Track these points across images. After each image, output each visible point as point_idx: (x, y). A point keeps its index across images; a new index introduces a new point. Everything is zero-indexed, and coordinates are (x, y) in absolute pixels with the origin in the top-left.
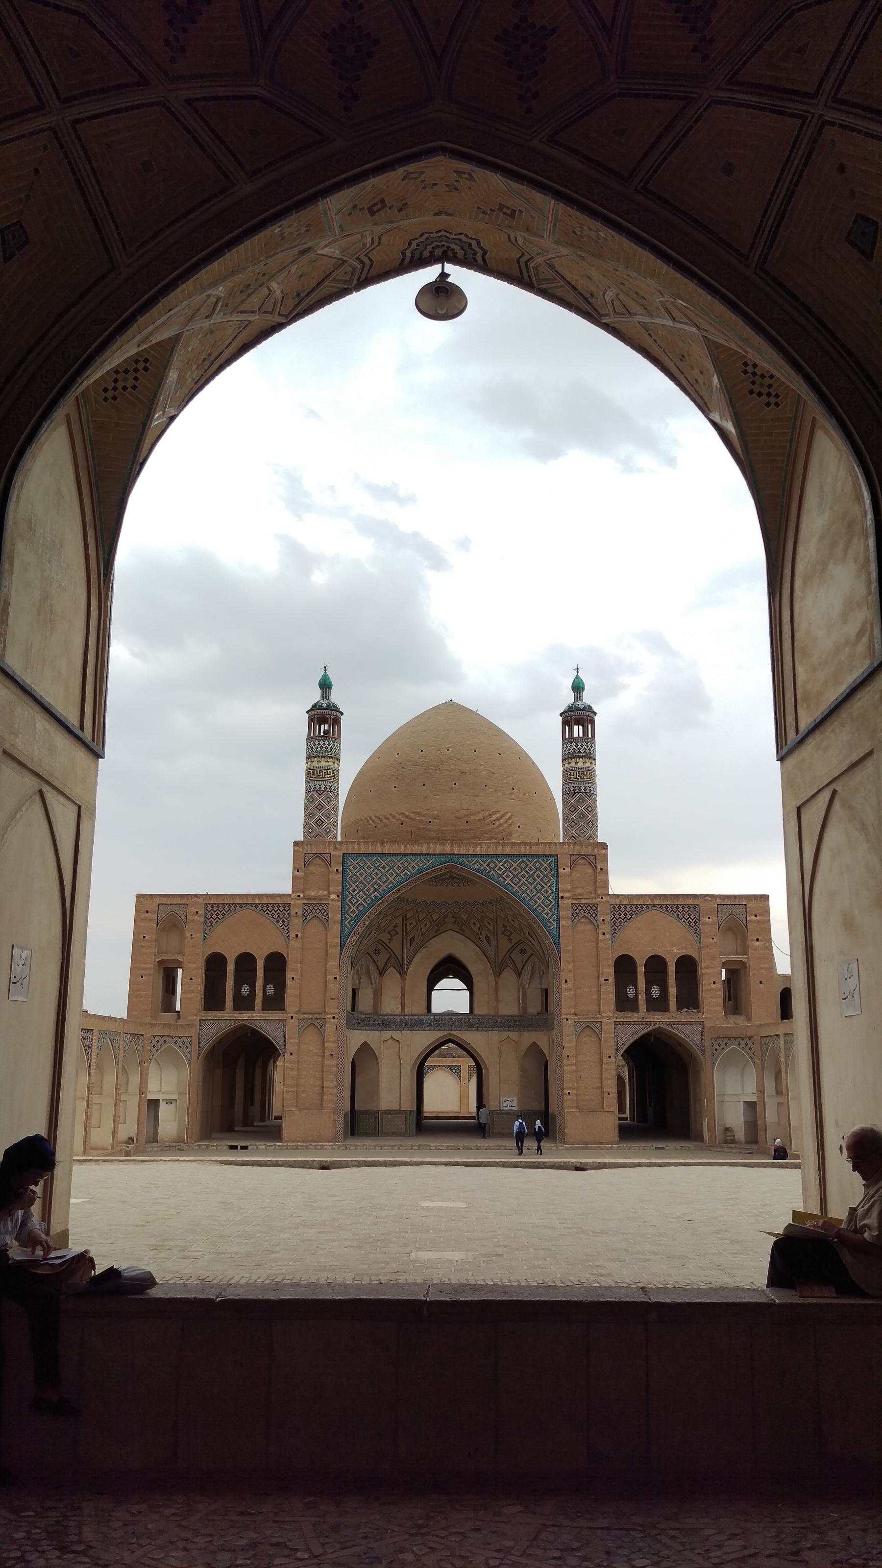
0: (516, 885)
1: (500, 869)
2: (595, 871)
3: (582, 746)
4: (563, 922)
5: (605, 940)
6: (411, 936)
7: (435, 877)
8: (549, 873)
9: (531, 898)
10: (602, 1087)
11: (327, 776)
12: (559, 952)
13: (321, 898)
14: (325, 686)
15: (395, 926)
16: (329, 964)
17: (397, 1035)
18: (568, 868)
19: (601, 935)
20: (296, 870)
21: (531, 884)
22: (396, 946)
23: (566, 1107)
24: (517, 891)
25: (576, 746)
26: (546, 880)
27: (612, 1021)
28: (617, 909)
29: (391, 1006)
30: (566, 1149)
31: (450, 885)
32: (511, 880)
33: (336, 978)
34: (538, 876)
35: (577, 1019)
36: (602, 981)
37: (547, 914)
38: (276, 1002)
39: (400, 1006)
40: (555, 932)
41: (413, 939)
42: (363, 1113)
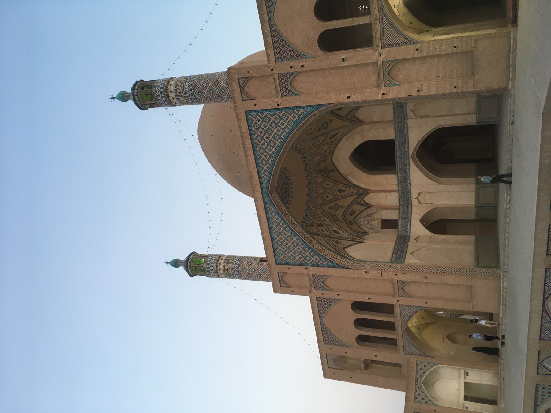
0: (275, 143)
1: (266, 156)
2: (252, 78)
3: (159, 95)
4: (298, 104)
5: (309, 65)
6: (337, 193)
7: (282, 200)
8: (260, 117)
9: (284, 130)
10: (448, 55)
11: (229, 270)
12: (324, 105)
13: (310, 279)
14: (176, 263)
15: (330, 208)
16: (356, 276)
17: (414, 195)
18: (254, 102)
19: (305, 68)
20: (293, 293)
21: (273, 131)
22: (346, 202)
23: (469, 90)
24: (280, 142)
25: (161, 100)
26: (267, 119)
27: (381, 51)
28: (279, 55)
29: (393, 199)
30: (514, 86)
31: (290, 181)
32: (273, 147)
33: (366, 272)
34: (265, 126)
35: (382, 86)
36: (345, 64)
37: (294, 117)
38: (388, 309)
39: (392, 193)
40: (308, 110)
41: (340, 191)
42: (477, 214)
